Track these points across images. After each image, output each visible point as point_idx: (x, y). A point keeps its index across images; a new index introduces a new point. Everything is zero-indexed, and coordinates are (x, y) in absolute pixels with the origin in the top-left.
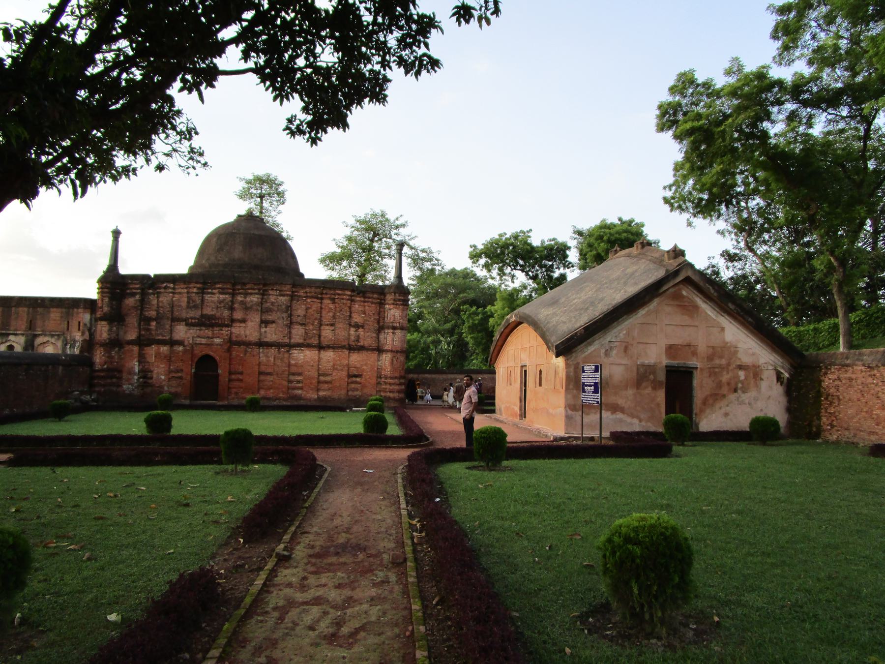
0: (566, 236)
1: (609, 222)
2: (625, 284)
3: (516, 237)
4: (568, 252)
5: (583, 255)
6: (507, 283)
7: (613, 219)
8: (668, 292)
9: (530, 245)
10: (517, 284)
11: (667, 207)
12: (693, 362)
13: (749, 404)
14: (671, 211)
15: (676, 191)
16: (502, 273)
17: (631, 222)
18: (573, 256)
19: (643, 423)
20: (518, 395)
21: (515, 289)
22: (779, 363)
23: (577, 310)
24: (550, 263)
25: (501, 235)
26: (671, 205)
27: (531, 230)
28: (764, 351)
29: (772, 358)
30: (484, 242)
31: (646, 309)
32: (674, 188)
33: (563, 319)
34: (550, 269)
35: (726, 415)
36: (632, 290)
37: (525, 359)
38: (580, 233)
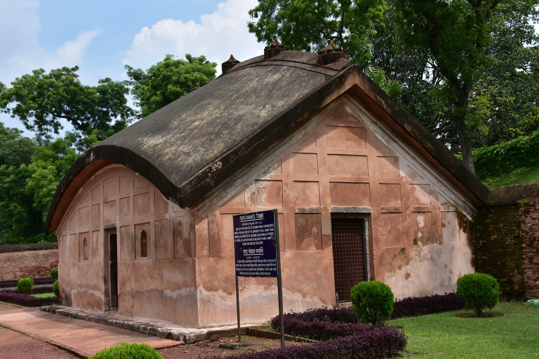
0: (120, 76)
1: (175, 59)
2: (269, 96)
3: (57, 75)
4: (126, 96)
5: (145, 102)
6: (49, 133)
7: (180, 56)
8: (328, 108)
9: (77, 85)
10: (62, 134)
11: (253, 36)
12: (365, 207)
14: (259, 41)
15: (263, 17)
16: (41, 122)
17: (202, 59)
18: (132, 101)
19: (308, 299)
20: (102, 274)
21: (59, 141)
22: (461, 203)
23: (203, 136)
24: (105, 109)
25: (35, 72)
26: (258, 35)
27: (76, 68)
28: (443, 188)
29: (453, 197)
30: (14, 80)
31: (303, 132)
32: (260, 14)
33: (185, 149)
34: (106, 117)
35: (408, 276)
36: (282, 105)
37: (112, 216)
38: (136, 75)
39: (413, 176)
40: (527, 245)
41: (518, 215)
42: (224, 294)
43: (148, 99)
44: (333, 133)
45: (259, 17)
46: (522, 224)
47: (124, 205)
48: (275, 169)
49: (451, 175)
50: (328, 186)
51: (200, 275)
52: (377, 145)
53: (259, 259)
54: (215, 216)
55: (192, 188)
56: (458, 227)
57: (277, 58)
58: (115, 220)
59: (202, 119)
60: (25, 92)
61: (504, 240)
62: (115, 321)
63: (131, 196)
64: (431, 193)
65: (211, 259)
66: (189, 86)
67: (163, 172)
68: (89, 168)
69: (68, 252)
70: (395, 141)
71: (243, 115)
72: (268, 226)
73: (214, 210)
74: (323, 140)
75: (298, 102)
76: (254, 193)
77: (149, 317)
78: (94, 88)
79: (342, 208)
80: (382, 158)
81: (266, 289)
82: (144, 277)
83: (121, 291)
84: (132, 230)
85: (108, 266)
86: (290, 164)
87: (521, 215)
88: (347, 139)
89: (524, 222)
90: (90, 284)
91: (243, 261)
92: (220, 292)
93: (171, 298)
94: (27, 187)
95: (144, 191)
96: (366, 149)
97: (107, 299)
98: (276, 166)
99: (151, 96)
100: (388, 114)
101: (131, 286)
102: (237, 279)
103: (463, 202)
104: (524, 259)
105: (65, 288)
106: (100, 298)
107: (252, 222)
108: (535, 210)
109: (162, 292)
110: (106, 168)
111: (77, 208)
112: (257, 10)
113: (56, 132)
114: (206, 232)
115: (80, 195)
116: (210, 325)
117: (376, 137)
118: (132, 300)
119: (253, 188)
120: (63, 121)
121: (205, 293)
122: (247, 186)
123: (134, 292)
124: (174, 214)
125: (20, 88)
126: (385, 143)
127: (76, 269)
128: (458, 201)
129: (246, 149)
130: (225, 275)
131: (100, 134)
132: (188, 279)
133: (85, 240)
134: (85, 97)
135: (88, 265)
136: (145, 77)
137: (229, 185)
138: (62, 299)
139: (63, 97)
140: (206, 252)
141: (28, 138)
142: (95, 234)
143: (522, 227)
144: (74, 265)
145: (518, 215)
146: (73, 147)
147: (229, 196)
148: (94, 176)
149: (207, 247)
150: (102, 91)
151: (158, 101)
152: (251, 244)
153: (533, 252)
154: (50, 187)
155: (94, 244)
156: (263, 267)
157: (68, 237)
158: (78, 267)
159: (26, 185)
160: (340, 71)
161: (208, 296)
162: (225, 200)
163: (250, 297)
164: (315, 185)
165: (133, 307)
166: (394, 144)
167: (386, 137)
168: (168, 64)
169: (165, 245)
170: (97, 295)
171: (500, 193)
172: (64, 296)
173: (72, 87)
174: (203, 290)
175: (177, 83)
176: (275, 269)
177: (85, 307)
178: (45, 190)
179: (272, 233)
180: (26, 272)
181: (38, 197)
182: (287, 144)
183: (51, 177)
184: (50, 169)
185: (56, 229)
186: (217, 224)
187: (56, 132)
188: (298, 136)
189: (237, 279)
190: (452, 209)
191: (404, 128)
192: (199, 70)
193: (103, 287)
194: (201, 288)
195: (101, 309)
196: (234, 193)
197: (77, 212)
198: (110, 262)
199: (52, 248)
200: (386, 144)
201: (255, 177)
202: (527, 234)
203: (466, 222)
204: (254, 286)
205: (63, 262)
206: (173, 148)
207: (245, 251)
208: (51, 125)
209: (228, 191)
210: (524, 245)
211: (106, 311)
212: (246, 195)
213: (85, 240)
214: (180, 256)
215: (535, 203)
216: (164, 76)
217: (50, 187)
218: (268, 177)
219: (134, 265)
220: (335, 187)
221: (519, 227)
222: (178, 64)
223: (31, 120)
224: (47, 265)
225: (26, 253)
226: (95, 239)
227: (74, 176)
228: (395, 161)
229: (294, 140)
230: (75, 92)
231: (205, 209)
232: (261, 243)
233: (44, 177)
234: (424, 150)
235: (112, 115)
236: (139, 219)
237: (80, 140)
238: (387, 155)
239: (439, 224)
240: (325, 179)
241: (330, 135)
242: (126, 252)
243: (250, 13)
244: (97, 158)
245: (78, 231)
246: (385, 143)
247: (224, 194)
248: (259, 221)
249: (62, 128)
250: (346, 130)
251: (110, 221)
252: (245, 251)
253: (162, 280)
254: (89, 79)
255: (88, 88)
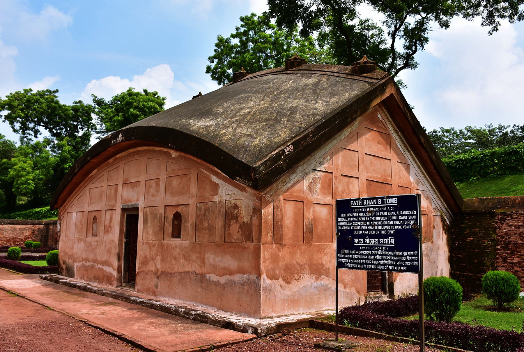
0: (88, 101)
1: (135, 91)
3: (41, 94)
6: (30, 137)
7: (138, 89)
9: (57, 102)
10: (40, 139)
16: (24, 127)
17: (155, 94)
19: (348, 290)
21: (38, 144)
22: (444, 209)
24: (75, 123)
25: (25, 90)
28: (435, 196)
29: (440, 203)
30: (8, 94)
31: (349, 130)
32: (216, 61)
34: (75, 129)
38: (99, 103)
39: (418, 182)
40: (501, 247)
41: (494, 222)
42: (283, 283)
43: (111, 118)
45: (215, 63)
46: (498, 230)
47: (150, 187)
48: (328, 161)
49: (443, 185)
51: (264, 262)
53: (386, 250)
54: (279, 201)
55: (266, 169)
56: (441, 229)
57: (299, 68)
58: (138, 200)
59: (252, 108)
60: (16, 103)
61: (481, 242)
62: (139, 300)
63: (163, 177)
65: (274, 246)
66: (145, 111)
67: (227, 151)
68: (111, 150)
69: (73, 228)
70: (408, 151)
71: (296, 107)
72: (406, 213)
73: (279, 195)
74: (363, 140)
75: (353, 100)
76: (312, 182)
77: (180, 299)
78: (69, 106)
81: (317, 279)
82: (175, 258)
83: (141, 270)
84: (161, 211)
85: (122, 244)
86: (339, 158)
87: (497, 222)
88: (378, 143)
89: (499, 228)
90: (99, 259)
91: (353, 252)
92: (280, 280)
93: (217, 284)
94: (8, 176)
95: (181, 173)
96: (391, 155)
97: (119, 275)
98: (328, 158)
99: (114, 116)
100: (411, 125)
101: (156, 266)
102: (337, 270)
103: (446, 209)
104: (498, 259)
105: (67, 260)
106: (111, 274)
107: (374, 208)
108: (512, 218)
109: (203, 276)
110: (131, 151)
111: (87, 188)
112: (215, 57)
113: (36, 136)
114: (271, 217)
115: (92, 176)
116: (270, 315)
118: (155, 280)
119: (311, 177)
120: (41, 129)
121: (268, 281)
122: (306, 174)
123: (160, 272)
124: (228, 197)
125: (13, 100)
127: (82, 244)
128: (442, 207)
129: (313, 137)
130: (285, 263)
131: (70, 141)
132: (246, 265)
133: (95, 218)
134: (63, 112)
135: (97, 242)
136: (106, 105)
138: (62, 269)
139: (45, 110)
140: (270, 238)
141: (9, 141)
142: (108, 213)
143: (498, 232)
144: (79, 240)
145: (494, 222)
146: (48, 148)
147: (292, 182)
148: (113, 158)
149: (271, 233)
150: (75, 109)
151: (119, 120)
152: (371, 232)
153: (507, 253)
154: (27, 177)
155: (107, 223)
156: (391, 260)
157: (74, 214)
158: (85, 242)
159: (7, 174)
160: (381, 80)
161: (270, 285)
162: (288, 185)
163: (304, 287)
164: (356, 180)
165: (157, 287)
166: (407, 153)
167: (403, 146)
168: (130, 94)
169: (211, 229)
170: (107, 271)
171: (474, 203)
172: (64, 267)
173: (53, 104)
174: (266, 278)
175: (136, 108)
176: (414, 263)
177: (90, 280)
178: (23, 179)
179: (413, 222)
180: (5, 241)
181: (17, 184)
182: (338, 139)
183: (29, 169)
184: (28, 164)
185: (61, 206)
186: (281, 210)
187: (36, 136)
189: (337, 270)
190: (439, 214)
191: (419, 140)
192: (152, 101)
193: (116, 264)
194: (264, 276)
195: (111, 284)
196: (295, 180)
197: (88, 192)
198: (125, 240)
199: (27, 224)
201: (312, 166)
202: (502, 238)
203: (446, 226)
204: (308, 276)
205: (66, 236)
206: (230, 130)
207: (356, 240)
208: (32, 131)
209: (291, 177)
210: (499, 247)
211: (117, 286)
212: (305, 183)
213: (95, 218)
214: (233, 241)
215: (512, 212)
216: (127, 102)
217: (27, 177)
218: (322, 168)
219: (162, 246)
220: (370, 185)
221: (495, 232)
222: (138, 94)
223: (17, 126)
224: (22, 237)
225: (6, 226)
226: (108, 217)
227: (93, 158)
228: (408, 168)
230: (55, 107)
231: (271, 194)
232: (392, 232)
233: (24, 169)
234: (429, 161)
235: (80, 128)
236: (172, 200)
237: (54, 144)
239: (432, 226)
240: (364, 177)
241: (367, 136)
242: (151, 232)
243: (209, 58)
244: (126, 139)
245: (87, 209)
246: (402, 150)
247: (288, 180)
248: (390, 207)
249: (41, 134)
250: (377, 134)
251: (130, 201)
252: (356, 240)
253: (204, 263)
254: (66, 100)
255: (65, 106)
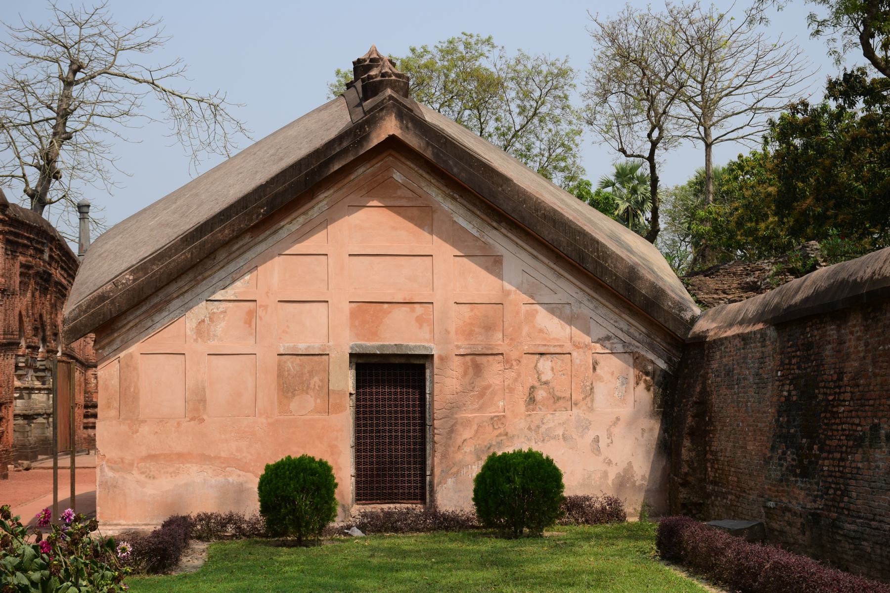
3: (449, 51)
13: (565, 438)
31: (301, 220)
44: (360, 217)
50: (347, 308)
52: (456, 237)
64: (570, 320)
76: (203, 321)
79: (373, 347)
80: (465, 259)
114: (115, 382)
116: (115, 522)
117: (455, 222)
121: (110, 474)
126: (474, 232)
137: (159, 308)
188: (290, 226)
200: (477, 234)
212: (188, 324)
229: (283, 233)
231: (115, 347)
238: (477, 253)
246: (474, 232)
247: (150, 324)
